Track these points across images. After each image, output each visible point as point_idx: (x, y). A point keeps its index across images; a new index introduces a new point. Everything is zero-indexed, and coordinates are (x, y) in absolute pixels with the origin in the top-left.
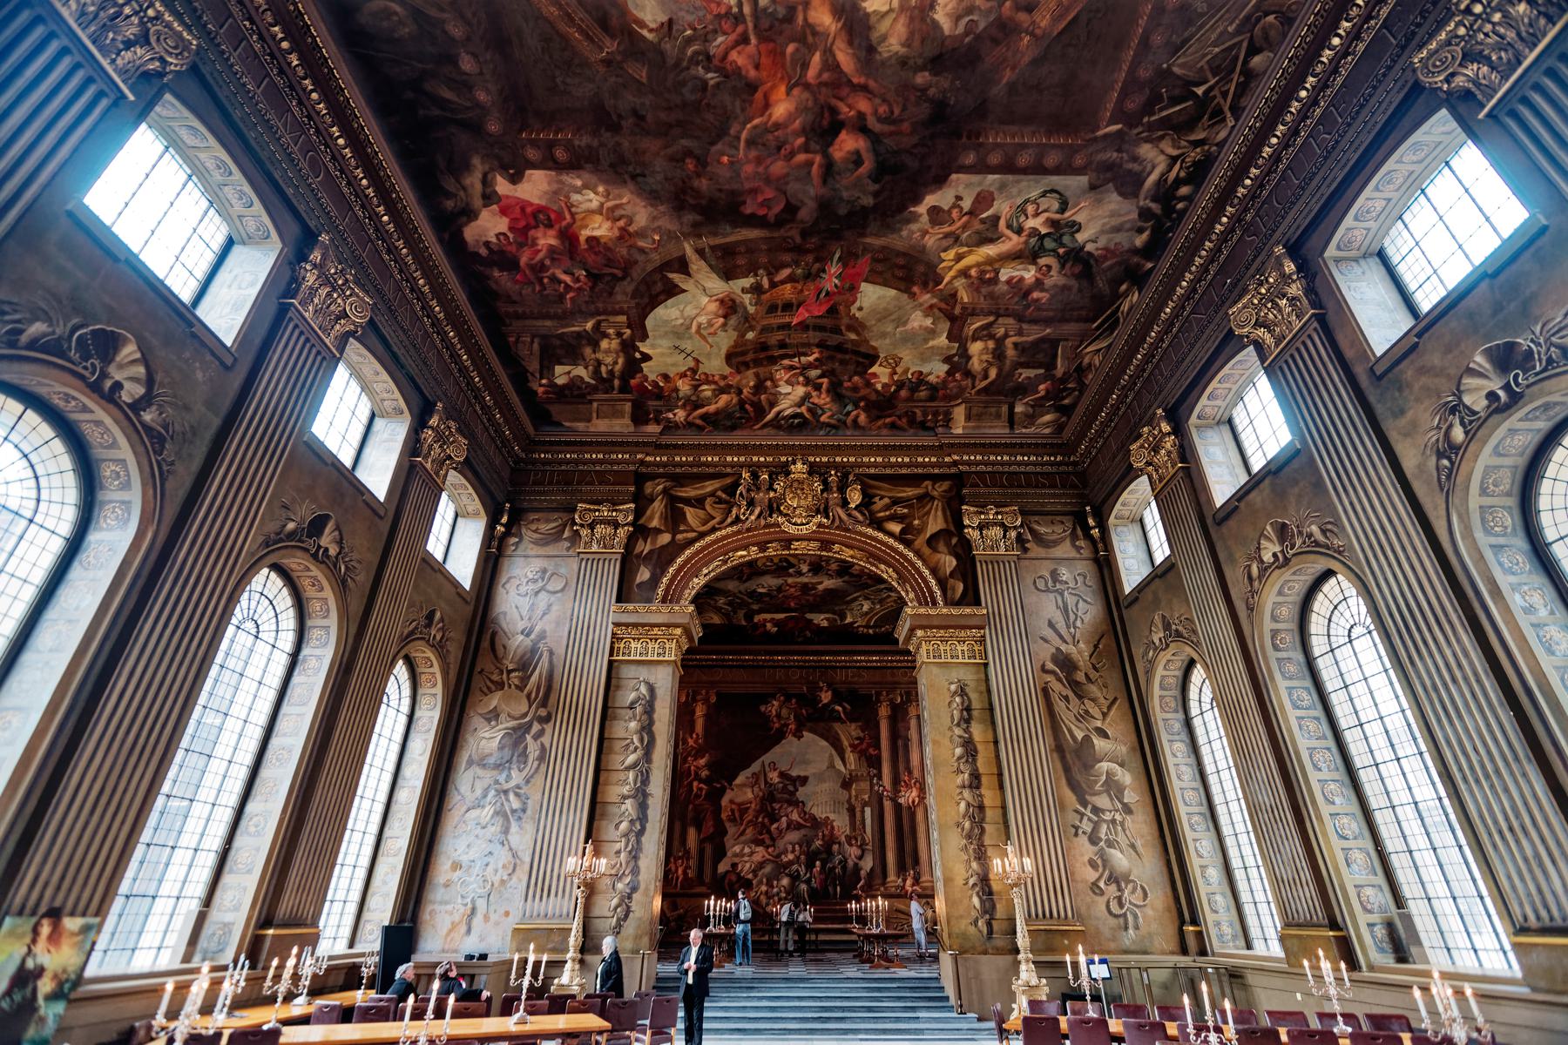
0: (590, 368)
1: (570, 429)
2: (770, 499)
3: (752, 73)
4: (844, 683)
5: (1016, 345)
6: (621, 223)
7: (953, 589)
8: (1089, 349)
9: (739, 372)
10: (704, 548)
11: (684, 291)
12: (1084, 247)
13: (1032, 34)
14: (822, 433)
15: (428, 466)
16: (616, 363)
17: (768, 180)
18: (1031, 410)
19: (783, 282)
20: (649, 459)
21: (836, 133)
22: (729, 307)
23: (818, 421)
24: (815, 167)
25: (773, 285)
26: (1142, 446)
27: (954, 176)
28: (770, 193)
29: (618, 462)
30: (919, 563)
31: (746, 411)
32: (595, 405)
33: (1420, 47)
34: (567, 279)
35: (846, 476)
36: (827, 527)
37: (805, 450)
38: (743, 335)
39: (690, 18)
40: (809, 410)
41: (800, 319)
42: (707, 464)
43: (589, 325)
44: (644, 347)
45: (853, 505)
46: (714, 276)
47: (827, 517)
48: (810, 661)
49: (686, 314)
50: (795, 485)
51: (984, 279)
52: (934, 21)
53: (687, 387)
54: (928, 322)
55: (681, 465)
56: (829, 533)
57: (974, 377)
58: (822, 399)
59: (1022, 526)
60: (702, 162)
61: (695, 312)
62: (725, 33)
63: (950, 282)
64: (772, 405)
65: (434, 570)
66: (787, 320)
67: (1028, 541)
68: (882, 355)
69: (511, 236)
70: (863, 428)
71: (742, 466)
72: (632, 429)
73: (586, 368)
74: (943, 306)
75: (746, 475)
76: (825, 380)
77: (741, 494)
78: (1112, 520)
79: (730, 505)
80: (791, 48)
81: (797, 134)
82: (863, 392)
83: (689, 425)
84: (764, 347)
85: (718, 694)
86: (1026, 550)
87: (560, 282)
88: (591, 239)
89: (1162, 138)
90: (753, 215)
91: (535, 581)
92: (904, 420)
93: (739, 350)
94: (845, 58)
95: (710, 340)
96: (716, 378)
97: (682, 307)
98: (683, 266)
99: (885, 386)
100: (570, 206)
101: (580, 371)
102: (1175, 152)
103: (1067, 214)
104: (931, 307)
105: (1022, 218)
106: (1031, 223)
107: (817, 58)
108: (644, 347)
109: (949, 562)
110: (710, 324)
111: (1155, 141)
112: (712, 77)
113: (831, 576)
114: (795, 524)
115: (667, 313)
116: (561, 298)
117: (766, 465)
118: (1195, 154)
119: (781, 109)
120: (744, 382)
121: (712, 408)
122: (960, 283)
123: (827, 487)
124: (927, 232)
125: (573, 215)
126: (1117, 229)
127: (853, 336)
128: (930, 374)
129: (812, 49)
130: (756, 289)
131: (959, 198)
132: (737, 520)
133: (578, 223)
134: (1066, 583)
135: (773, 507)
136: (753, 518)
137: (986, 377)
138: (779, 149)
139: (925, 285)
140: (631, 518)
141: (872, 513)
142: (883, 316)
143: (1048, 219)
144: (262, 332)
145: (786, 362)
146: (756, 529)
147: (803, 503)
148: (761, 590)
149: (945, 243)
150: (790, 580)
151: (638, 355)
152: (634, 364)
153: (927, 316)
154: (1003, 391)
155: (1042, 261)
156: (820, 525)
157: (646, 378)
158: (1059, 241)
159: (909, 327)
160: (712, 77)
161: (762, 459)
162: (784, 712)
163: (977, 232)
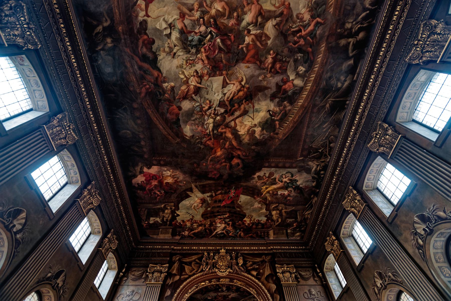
0: (161, 218)
1: (152, 238)
2: (213, 262)
3: (212, 146)
5: (285, 212)
6: (176, 179)
7: (276, 298)
8: (306, 213)
9: (205, 220)
10: (190, 282)
11: (191, 197)
12: (299, 186)
13: (278, 139)
14: (230, 239)
15: (103, 251)
16: (169, 217)
17: (215, 169)
18: (292, 231)
19: (219, 194)
20: (175, 248)
21: (233, 159)
22: (203, 201)
23: (229, 235)
24: (227, 166)
25: (216, 195)
26: (328, 244)
27: (263, 169)
28: (216, 172)
29: (165, 249)
30: (263, 288)
31: (207, 232)
32: (161, 230)
33: (368, 143)
34: (158, 193)
35: (237, 254)
36: (232, 273)
37: (225, 245)
38: (207, 209)
39: (198, 135)
40: (226, 231)
41: (223, 204)
42: (194, 250)
43: (163, 206)
44: (178, 212)
45: (240, 265)
46: (200, 193)
47: (232, 269)
50: (221, 257)
51: (274, 194)
52: (255, 136)
53: (189, 224)
54: (260, 205)
55: (185, 250)
56: (232, 276)
57: (274, 221)
58: (230, 228)
59: (296, 272)
60: (198, 165)
62: (206, 138)
63: (265, 195)
64: (215, 230)
65: (95, 291)
66: (220, 205)
67: (299, 278)
68: (247, 215)
69: (145, 182)
70: (243, 238)
71: (204, 250)
72: (171, 238)
73: (160, 218)
74: (263, 201)
75: (206, 254)
76: (231, 222)
77: (204, 260)
78: (325, 270)
79: (200, 265)
80: (221, 141)
81: (223, 159)
82: (242, 226)
83: (189, 236)
84: (212, 212)
86: (299, 282)
87: (156, 194)
88: (167, 183)
89: (314, 160)
90: (211, 177)
91: (129, 296)
92: (255, 235)
94: (234, 143)
95: (197, 210)
96: (198, 222)
97: (190, 201)
98: (191, 190)
99: (248, 224)
100: (162, 174)
101: (158, 219)
102: (318, 164)
103: (294, 178)
104: (260, 201)
105: (282, 179)
106: (284, 180)
107: (228, 143)
108: (178, 212)
109: (274, 287)
110: (198, 206)
111: (312, 161)
112: (202, 147)
113: (233, 292)
114: (221, 272)
115: (186, 202)
116: (156, 198)
117: (212, 250)
118: (323, 164)
119: (219, 153)
120: (207, 223)
121: (196, 231)
122: (267, 195)
123: (232, 259)
124: (257, 182)
125: (163, 177)
126: (307, 181)
127: (239, 209)
128: (262, 220)
129: (227, 141)
130: (211, 196)
131: (265, 174)
132: (202, 271)
133: (164, 179)
134: (314, 295)
135: (214, 265)
136: (207, 269)
137: (278, 221)
138: (218, 162)
139: (258, 196)
140: (166, 270)
141: (247, 268)
142: (247, 203)
143: (289, 179)
144: (66, 208)
145: (219, 217)
146: (208, 274)
147: (224, 264)
148: (209, 298)
149: (263, 185)
150: (219, 294)
151: (176, 215)
152: (174, 217)
153: (259, 204)
154: (283, 226)
155: (289, 189)
156: (230, 272)
157: (177, 221)
158: (292, 184)
159: (254, 207)
160: (202, 147)
161: (211, 248)
163: (271, 182)
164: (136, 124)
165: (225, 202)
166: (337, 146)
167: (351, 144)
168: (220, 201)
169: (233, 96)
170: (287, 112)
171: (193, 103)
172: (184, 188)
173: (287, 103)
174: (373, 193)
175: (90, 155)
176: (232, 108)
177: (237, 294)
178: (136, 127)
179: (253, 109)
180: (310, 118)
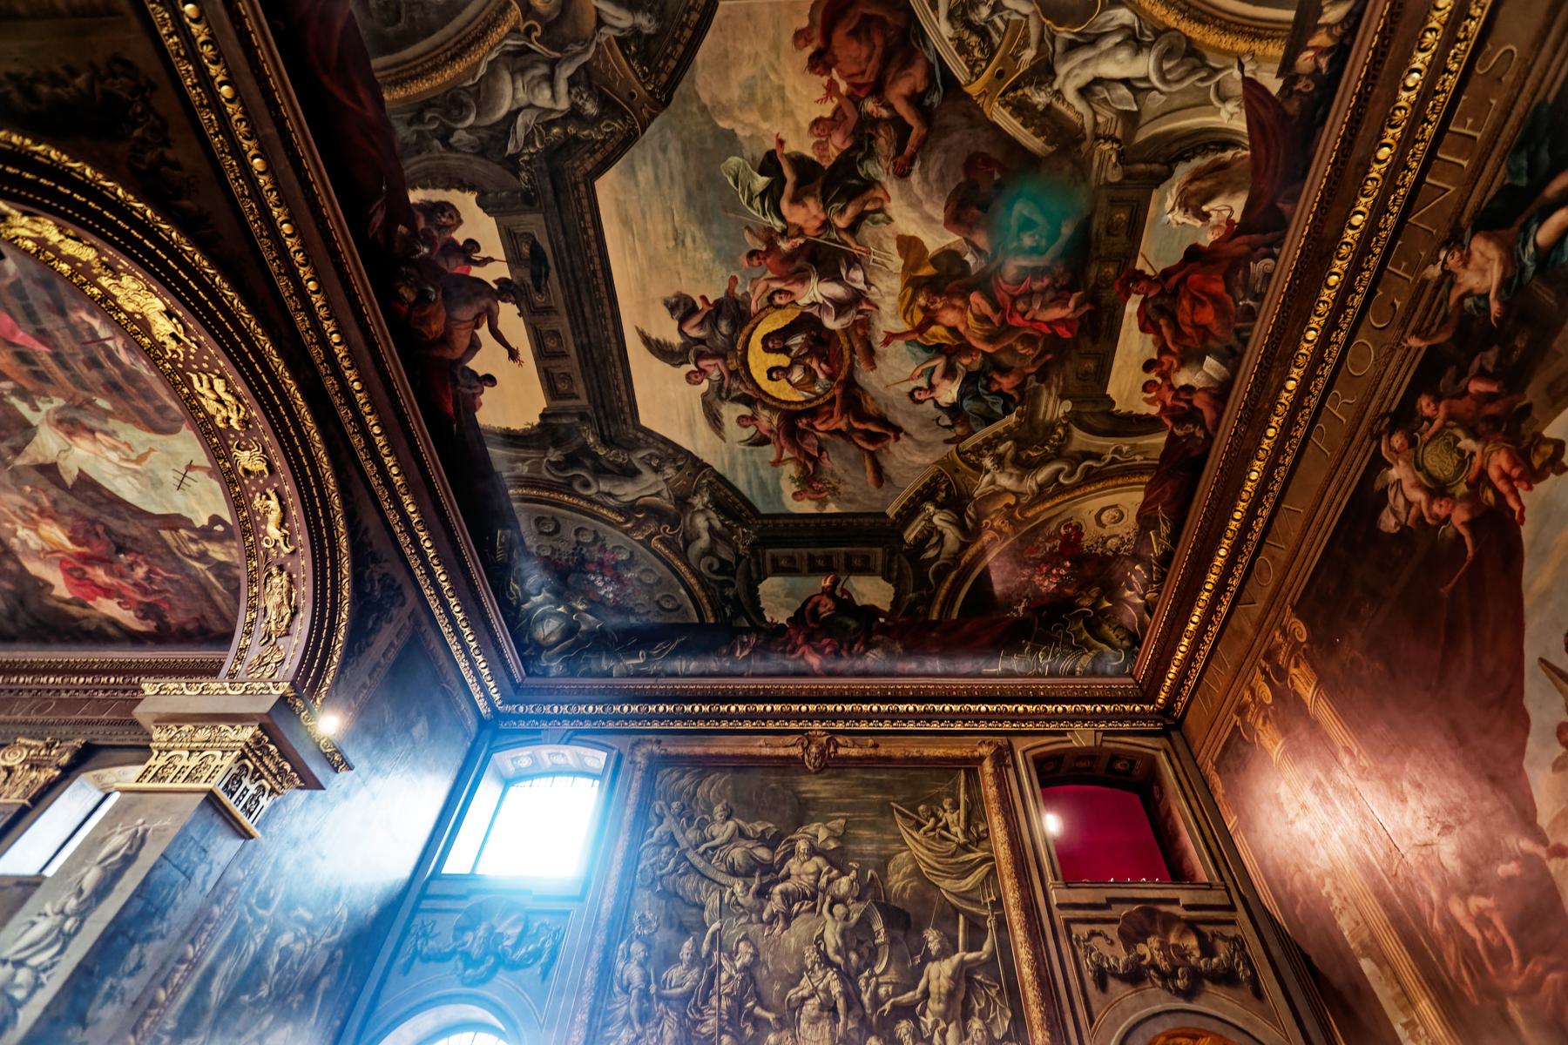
4: (1478, 170)
11: (80, 470)
22: (70, 425)
34: (140, 572)
43: (197, 565)
46: (37, 438)
48: (1347, 288)
49: (117, 472)
61: (104, 461)
84: (112, 388)
85: (1297, 610)
93: (137, 418)
95: (142, 451)
98: (49, 471)
108: (202, 520)
110: (115, 448)
115: (127, 489)
130: (22, 393)
150: (889, 319)
162: (1438, 462)
165: (13, 333)
168: (23, 357)
172: (54, 492)
177: (892, 187)
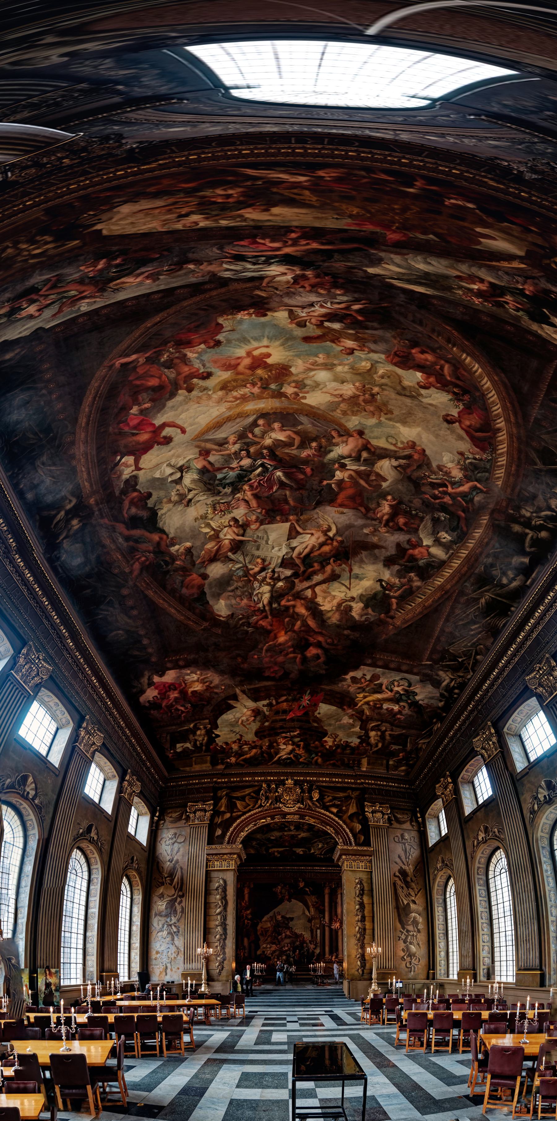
37: (292, 775)
81: (289, 647)
113: (304, 832)
164: (130, 617)
166: (486, 661)
167: (505, 666)
169: (312, 551)
170: (414, 589)
171: (230, 566)
173: (415, 576)
174: (513, 739)
175: (73, 682)
176: (307, 569)
178: (129, 621)
179: (350, 572)
180: (453, 608)
